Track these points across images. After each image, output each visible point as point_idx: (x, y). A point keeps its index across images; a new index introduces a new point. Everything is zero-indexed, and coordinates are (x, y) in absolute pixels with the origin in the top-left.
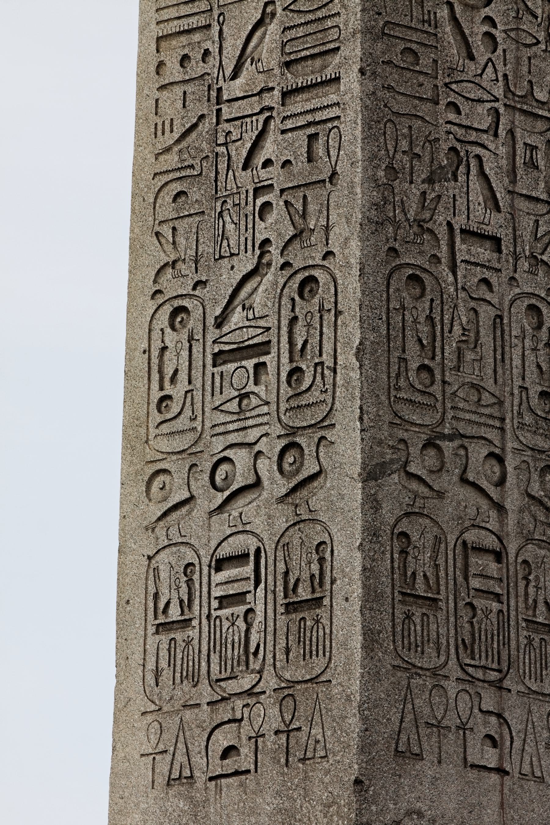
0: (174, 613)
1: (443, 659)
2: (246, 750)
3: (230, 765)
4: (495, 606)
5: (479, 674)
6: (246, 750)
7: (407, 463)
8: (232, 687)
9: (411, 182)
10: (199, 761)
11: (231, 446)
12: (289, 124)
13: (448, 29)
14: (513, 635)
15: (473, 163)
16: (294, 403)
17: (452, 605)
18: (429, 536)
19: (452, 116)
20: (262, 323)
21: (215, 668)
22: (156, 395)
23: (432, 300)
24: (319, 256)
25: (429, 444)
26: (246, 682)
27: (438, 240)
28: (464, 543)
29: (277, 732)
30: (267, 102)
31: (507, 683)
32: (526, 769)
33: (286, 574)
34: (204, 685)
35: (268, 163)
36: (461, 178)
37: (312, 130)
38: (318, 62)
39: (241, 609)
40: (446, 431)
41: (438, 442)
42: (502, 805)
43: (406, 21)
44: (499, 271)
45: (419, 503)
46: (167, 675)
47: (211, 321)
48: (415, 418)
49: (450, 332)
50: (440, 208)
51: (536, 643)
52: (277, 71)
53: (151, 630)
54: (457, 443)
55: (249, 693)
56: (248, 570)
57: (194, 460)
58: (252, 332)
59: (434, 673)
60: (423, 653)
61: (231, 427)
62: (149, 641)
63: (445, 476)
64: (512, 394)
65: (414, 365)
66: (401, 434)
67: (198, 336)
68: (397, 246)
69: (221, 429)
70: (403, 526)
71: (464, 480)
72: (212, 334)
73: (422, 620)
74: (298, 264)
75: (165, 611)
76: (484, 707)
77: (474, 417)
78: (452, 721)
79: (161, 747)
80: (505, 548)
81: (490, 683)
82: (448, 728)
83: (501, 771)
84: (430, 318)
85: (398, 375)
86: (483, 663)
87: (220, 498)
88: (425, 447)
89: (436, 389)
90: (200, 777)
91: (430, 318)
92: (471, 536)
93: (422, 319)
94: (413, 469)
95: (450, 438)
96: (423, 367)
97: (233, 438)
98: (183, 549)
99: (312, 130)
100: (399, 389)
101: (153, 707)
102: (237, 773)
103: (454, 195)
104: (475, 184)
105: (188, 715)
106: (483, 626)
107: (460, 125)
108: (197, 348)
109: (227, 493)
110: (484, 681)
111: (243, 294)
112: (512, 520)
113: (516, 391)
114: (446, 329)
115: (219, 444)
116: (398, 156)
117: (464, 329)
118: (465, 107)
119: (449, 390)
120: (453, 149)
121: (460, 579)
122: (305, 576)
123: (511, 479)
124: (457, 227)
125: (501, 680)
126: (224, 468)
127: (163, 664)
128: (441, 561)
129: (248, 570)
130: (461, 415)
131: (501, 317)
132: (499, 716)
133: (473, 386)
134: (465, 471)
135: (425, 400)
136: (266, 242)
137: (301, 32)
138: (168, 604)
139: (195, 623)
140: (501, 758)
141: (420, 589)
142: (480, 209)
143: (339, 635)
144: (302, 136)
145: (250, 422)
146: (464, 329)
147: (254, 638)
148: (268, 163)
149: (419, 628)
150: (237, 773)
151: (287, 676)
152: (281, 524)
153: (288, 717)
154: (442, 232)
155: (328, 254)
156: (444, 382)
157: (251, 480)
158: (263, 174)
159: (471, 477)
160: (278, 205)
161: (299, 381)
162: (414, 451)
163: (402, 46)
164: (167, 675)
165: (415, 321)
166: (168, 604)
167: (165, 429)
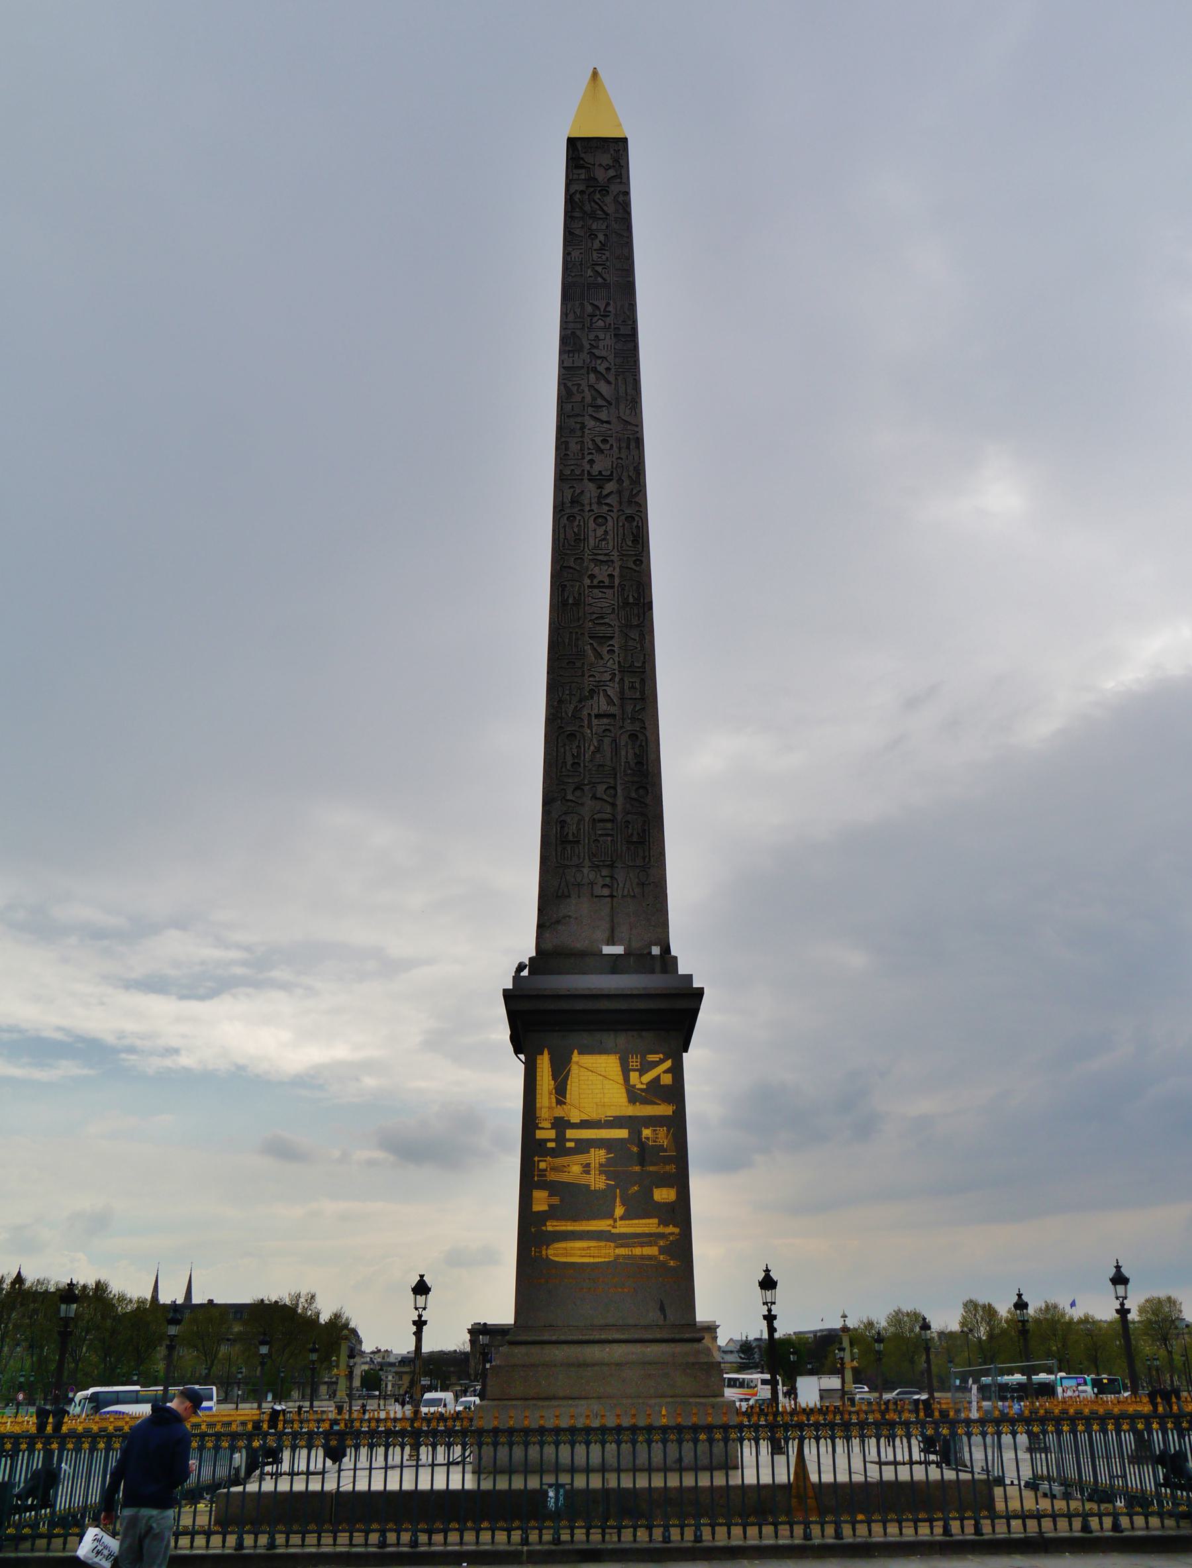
1: (581, 860)
4: (609, 839)
5: (601, 864)
9: (570, 703)
13: (590, 652)
14: (619, 847)
17: (587, 841)
19: (591, 679)
23: (579, 741)
25: (575, 789)
27: (583, 720)
28: (594, 819)
31: (616, 865)
32: (625, 893)
41: (582, 787)
42: (612, 908)
43: (570, 653)
44: (613, 725)
48: (570, 781)
49: (588, 749)
59: (577, 866)
60: (571, 860)
64: (621, 765)
65: (569, 763)
66: (562, 787)
68: (563, 725)
71: (594, 797)
73: (571, 850)
76: (603, 874)
77: (599, 776)
80: (616, 819)
81: (608, 866)
83: (612, 896)
84: (579, 747)
85: (562, 768)
86: (603, 859)
91: (579, 747)
93: (574, 747)
94: (568, 798)
95: (587, 785)
96: (574, 763)
100: (562, 772)
103: (592, 705)
104: (603, 700)
106: (603, 846)
110: (604, 866)
113: (623, 764)
114: (586, 749)
117: (595, 747)
119: (587, 769)
124: (593, 715)
125: (613, 864)
128: (582, 827)
132: (612, 877)
133: (600, 765)
141: (571, 838)
146: (595, 747)
149: (569, 852)
156: (585, 766)
159: (598, 796)
162: (569, 792)
163: (567, 661)
165: (571, 749)
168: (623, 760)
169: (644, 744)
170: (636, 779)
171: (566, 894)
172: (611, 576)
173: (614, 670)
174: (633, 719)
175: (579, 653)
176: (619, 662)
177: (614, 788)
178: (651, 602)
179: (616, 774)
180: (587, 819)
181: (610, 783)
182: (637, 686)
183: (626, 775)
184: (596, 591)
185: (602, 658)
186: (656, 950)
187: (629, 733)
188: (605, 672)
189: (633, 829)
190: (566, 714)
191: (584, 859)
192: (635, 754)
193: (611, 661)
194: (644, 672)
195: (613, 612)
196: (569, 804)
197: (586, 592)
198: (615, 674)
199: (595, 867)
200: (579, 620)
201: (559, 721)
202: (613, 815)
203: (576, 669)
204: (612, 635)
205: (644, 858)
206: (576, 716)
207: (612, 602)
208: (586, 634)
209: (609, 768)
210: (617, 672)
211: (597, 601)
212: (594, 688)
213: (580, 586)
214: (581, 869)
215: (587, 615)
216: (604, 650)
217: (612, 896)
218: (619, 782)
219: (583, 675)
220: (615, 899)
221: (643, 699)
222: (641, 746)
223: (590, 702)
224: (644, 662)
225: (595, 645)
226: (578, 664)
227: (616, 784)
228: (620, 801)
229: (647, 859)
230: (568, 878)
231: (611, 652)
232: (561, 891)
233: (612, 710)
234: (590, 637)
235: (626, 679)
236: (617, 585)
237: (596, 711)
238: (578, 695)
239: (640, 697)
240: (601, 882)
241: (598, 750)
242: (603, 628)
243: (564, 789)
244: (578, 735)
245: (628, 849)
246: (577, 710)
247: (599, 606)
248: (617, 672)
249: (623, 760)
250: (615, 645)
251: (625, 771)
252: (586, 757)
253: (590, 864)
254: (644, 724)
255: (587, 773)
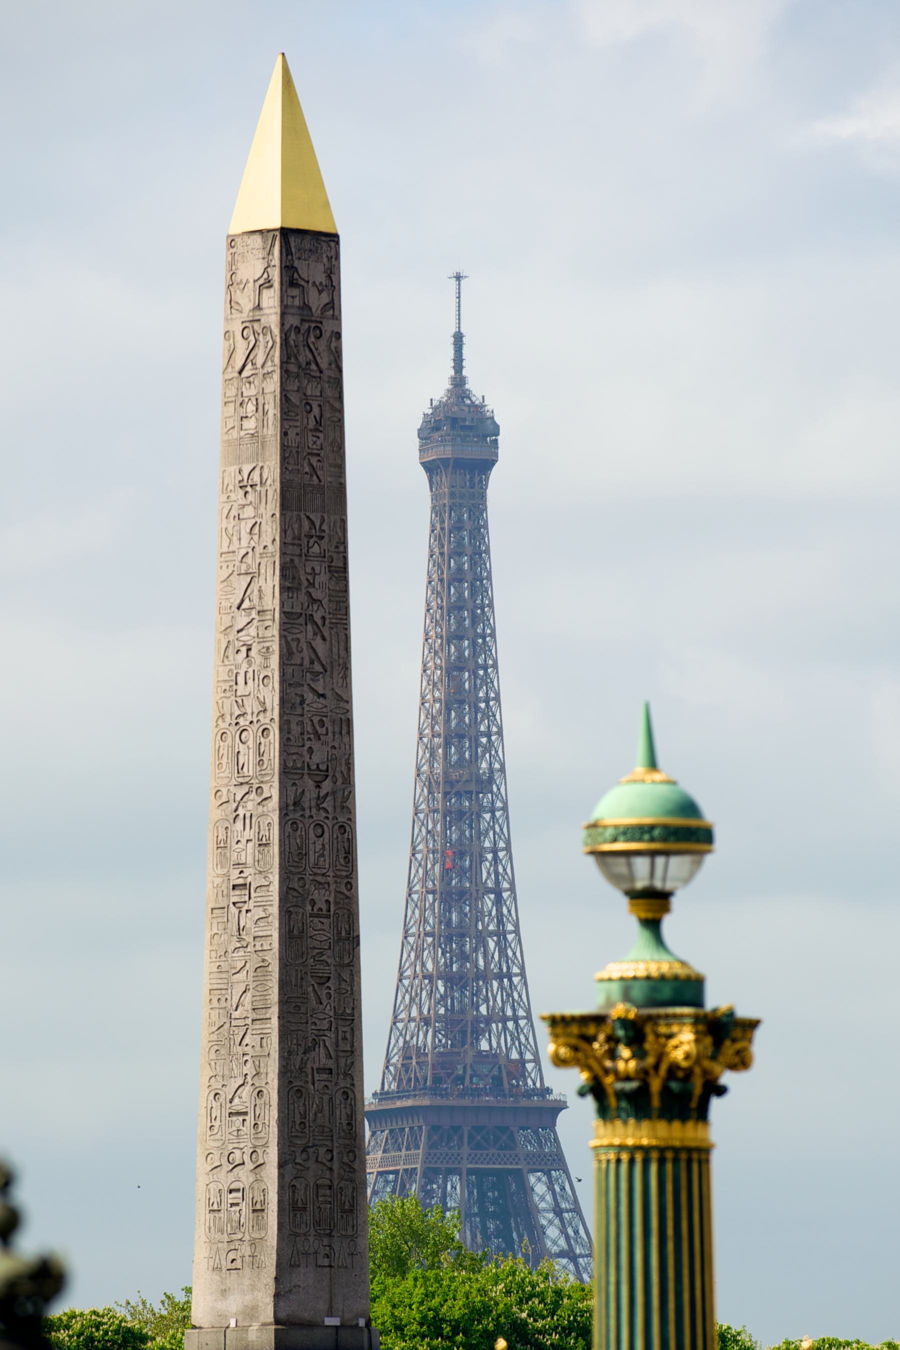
0: (215, 1207)
2: (239, 1261)
3: (234, 1266)
4: (329, 1206)
5: (322, 1232)
6: (239, 1261)
7: (295, 1159)
8: (234, 1237)
10: (223, 1262)
11: (234, 1148)
12: (254, 1032)
15: (321, 1043)
16: (256, 1136)
18: (304, 1185)
19: (313, 1027)
20: (245, 1104)
21: (229, 1229)
22: (209, 1125)
24: (264, 1083)
26: (240, 1236)
28: (317, 1185)
29: (249, 1256)
30: (247, 1022)
31: (333, 1234)
32: (340, 1264)
33: (253, 1198)
34: (225, 1235)
35: (247, 1045)
36: (317, 1050)
37: (262, 1036)
38: (264, 1011)
39: (237, 1208)
40: (310, 1145)
42: (331, 1278)
44: (331, 1081)
45: (299, 1172)
46: (213, 1229)
47: (228, 1100)
48: (298, 1142)
50: (309, 1062)
51: (345, 1217)
52: (250, 1011)
53: (208, 1212)
54: (314, 1148)
55: (240, 1240)
56: (240, 1195)
57: (222, 1151)
58: (242, 1107)
59: (305, 1234)
61: (235, 1141)
62: (207, 1215)
63: (309, 1161)
65: (298, 1122)
66: (293, 1149)
67: (224, 1105)
69: (231, 1141)
70: (294, 1183)
72: (229, 1105)
74: (257, 1085)
75: (212, 1205)
77: (321, 1138)
78: (312, 1250)
79: (211, 1256)
82: (310, 1254)
83: (330, 1266)
84: (304, 1104)
85: (292, 1128)
87: (231, 1166)
88: (302, 1152)
89: (307, 1130)
90: (224, 1269)
91: (304, 1104)
92: (319, 1182)
93: (301, 1105)
94: (297, 1161)
95: (312, 1147)
96: (301, 1123)
97: (235, 1145)
98: (218, 1183)
99: (262, 1036)
100: (292, 1133)
101: (208, 1240)
102: (236, 1269)
104: (322, 1051)
105: (220, 1245)
107: (316, 1030)
108: (223, 1109)
109: (233, 1165)
111: (239, 1092)
112: (336, 1172)
115: (230, 1147)
116: (293, 1046)
118: (318, 1022)
119: (311, 1129)
120: (314, 1039)
121: (315, 1198)
122: (259, 1200)
123: (335, 1158)
124: (315, 1068)
126: (232, 1155)
127: (212, 1225)
129: (240, 1195)
130: (316, 1138)
131: (332, 1098)
132: (330, 1246)
134: (317, 1158)
135: (303, 1135)
136: (246, 1074)
137: (258, 998)
138: (213, 1203)
139: (222, 1211)
140: (330, 1262)
142: (324, 1060)
143: (270, 1223)
144: (258, 1038)
145: (241, 1141)
147: (242, 1221)
148: (247, 1045)
150: (236, 1269)
151: (253, 1236)
152: (251, 1179)
153: (253, 1251)
154: (309, 1071)
155: (267, 1083)
156: (309, 1126)
157: (241, 1162)
158: (246, 1049)
159: (320, 1160)
160: (250, 1061)
161: (257, 1128)
162: (298, 1154)
164: (213, 1229)
165: (299, 1106)
166: (213, 1203)
167: (212, 1137)
168: (338, 1121)
169: (353, 1103)
170: (347, 1142)
171: (298, 1263)
172: (327, 901)
173: (331, 1017)
174: (346, 1074)
175: (304, 996)
176: (334, 1007)
177: (331, 1151)
178: (358, 936)
179: (332, 1136)
180: (312, 1184)
181: (327, 1146)
182: (349, 1037)
183: (339, 1138)
184: (316, 920)
185: (321, 1003)
186: (362, 1322)
187: (342, 1090)
188: (325, 1019)
189: (345, 1196)
190: (295, 1067)
191: (310, 1227)
192: (347, 1113)
193: (328, 1006)
194: (353, 1020)
195: (330, 948)
196: (298, 1167)
197: (308, 921)
198: (331, 1021)
199: (318, 1236)
200: (303, 954)
201: (289, 1074)
202: (331, 1181)
203: (301, 1015)
204: (329, 975)
205: (353, 1227)
206: (301, 1069)
207: (329, 935)
208: (309, 974)
209: (328, 1130)
210: (333, 1020)
211: (317, 933)
212: (316, 1038)
213: (303, 914)
214: (309, 1238)
215: (310, 950)
216: (323, 993)
217: (330, 1266)
218: (336, 1145)
219: (307, 1023)
220: (333, 1269)
221: (352, 1052)
222: (351, 1105)
223: (313, 1054)
224: (353, 1009)
225: (316, 986)
226: (303, 1010)
227: (332, 1148)
228: (336, 1166)
229: (355, 1228)
230: (298, 1246)
231: (329, 996)
232: (293, 1259)
233: (331, 1064)
234: (312, 976)
235: (339, 1027)
236: (332, 913)
237: (316, 1065)
238: (303, 1045)
239: (350, 1049)
240: (324, 1251)
241: (320, 1110)
242: (322, 967)
243: (293, 1151)
244: (303, 1090)
245: (342, 1217)
246: (303, 1063)
247: (319, 939)
248: (333, 1020)
249: (338, 1121)
250: (332, 989)
251: (339, 1133)
252: (311, 1114)
253: (315, 1233)
254: (353, 1080)
255: (311, 1135)
